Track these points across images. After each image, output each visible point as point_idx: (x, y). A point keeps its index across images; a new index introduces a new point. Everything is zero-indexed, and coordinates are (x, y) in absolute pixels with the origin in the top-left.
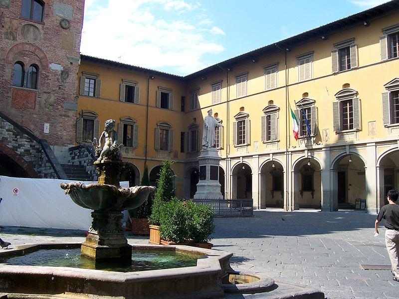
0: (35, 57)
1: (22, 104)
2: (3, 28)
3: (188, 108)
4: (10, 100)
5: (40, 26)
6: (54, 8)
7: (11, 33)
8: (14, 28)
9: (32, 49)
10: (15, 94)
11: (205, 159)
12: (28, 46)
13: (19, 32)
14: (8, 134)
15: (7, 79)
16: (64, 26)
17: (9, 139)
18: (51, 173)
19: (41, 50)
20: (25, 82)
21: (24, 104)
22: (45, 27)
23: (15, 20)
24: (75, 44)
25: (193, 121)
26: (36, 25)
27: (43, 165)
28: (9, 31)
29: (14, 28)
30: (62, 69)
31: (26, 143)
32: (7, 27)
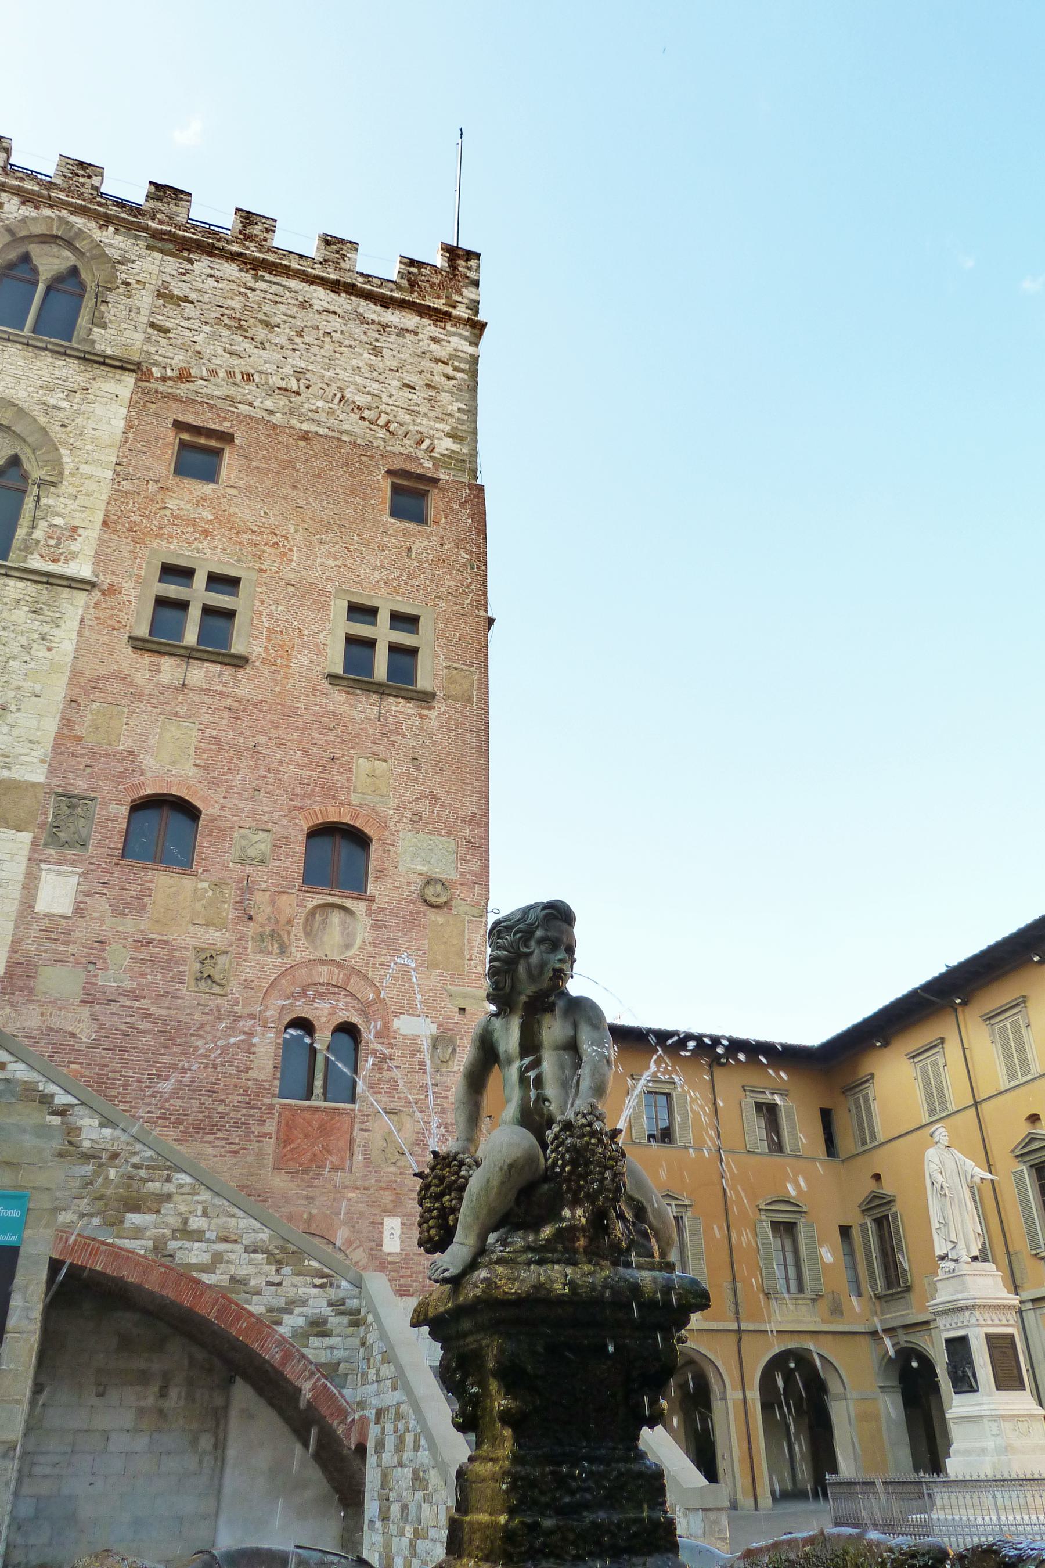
0: (349, 999)
1: (308, 1156)
2: (251, 924)
3: (846, 1143)
4: (270, 1146)
5: (359, 907)
6: (400, 850)
7: (274, 935)
8: (283, 921)
9: (338, 976)
10: (287, 1125)
11: (960, 1309)
12: (325, 969)
13: (298, 930)
14: (251, 1263)
15: (261, 1077)
16: (433, 900)
17: (252, 1283)
18: (398, 1405)
19: (364, 977)
20: (318, 1083)
21: (315, 1155)
22: (374, 907)
23: (285, 897)
24: (471, 948)
25: (871, 1185)
26: (348, 903)
27: (372, 1375)
28: (268, 929)
29: (283, 921)
30: (433, 1030)
31: (315, 1291)
32: (260, 918)
